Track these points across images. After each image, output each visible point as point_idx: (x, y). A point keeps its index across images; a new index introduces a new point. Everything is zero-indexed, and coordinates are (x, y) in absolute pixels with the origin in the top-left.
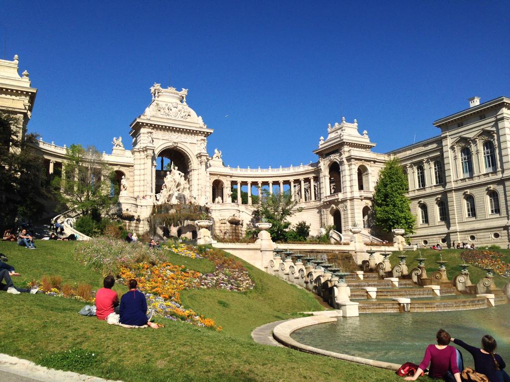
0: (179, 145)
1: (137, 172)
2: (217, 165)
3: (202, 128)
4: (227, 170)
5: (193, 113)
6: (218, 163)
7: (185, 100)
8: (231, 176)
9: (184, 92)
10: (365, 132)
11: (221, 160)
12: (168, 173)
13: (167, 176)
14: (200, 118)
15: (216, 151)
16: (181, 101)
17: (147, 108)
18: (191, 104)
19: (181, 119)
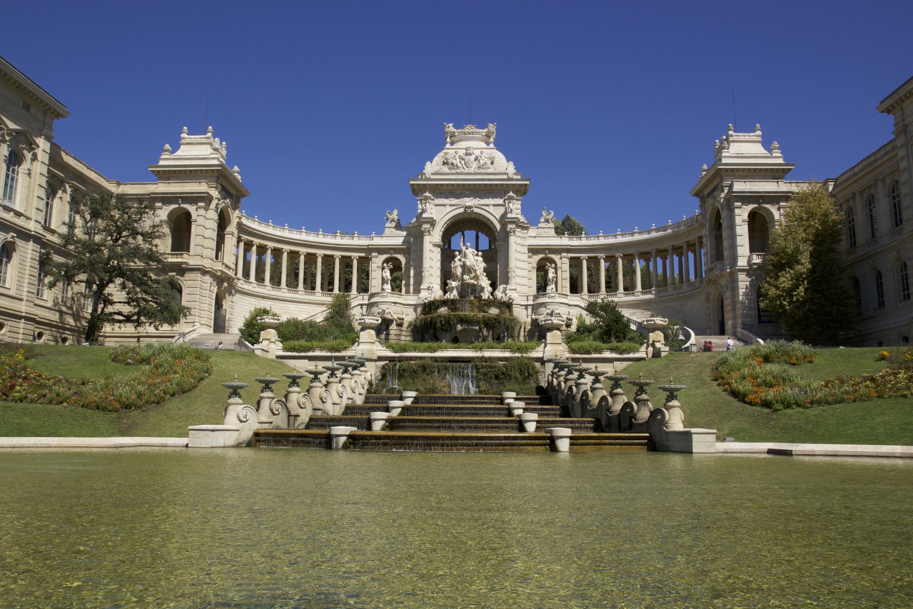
0: (476, 210)
1: (413, 256)
2: (545, 235)
3: (512, 179)
4: (564, 241)
5: (499, 157)
6: (547, 230)
7: (492, 140)
8: (568, 250)
9: (492, 127)
10: (776, 144)
11: (552, 225)
13: (456, 259)
14: (511, 164)
15: (544, 214)
16: (488, 144)
17: (428, 163)
18: (499, 147)
19: (481, 171)
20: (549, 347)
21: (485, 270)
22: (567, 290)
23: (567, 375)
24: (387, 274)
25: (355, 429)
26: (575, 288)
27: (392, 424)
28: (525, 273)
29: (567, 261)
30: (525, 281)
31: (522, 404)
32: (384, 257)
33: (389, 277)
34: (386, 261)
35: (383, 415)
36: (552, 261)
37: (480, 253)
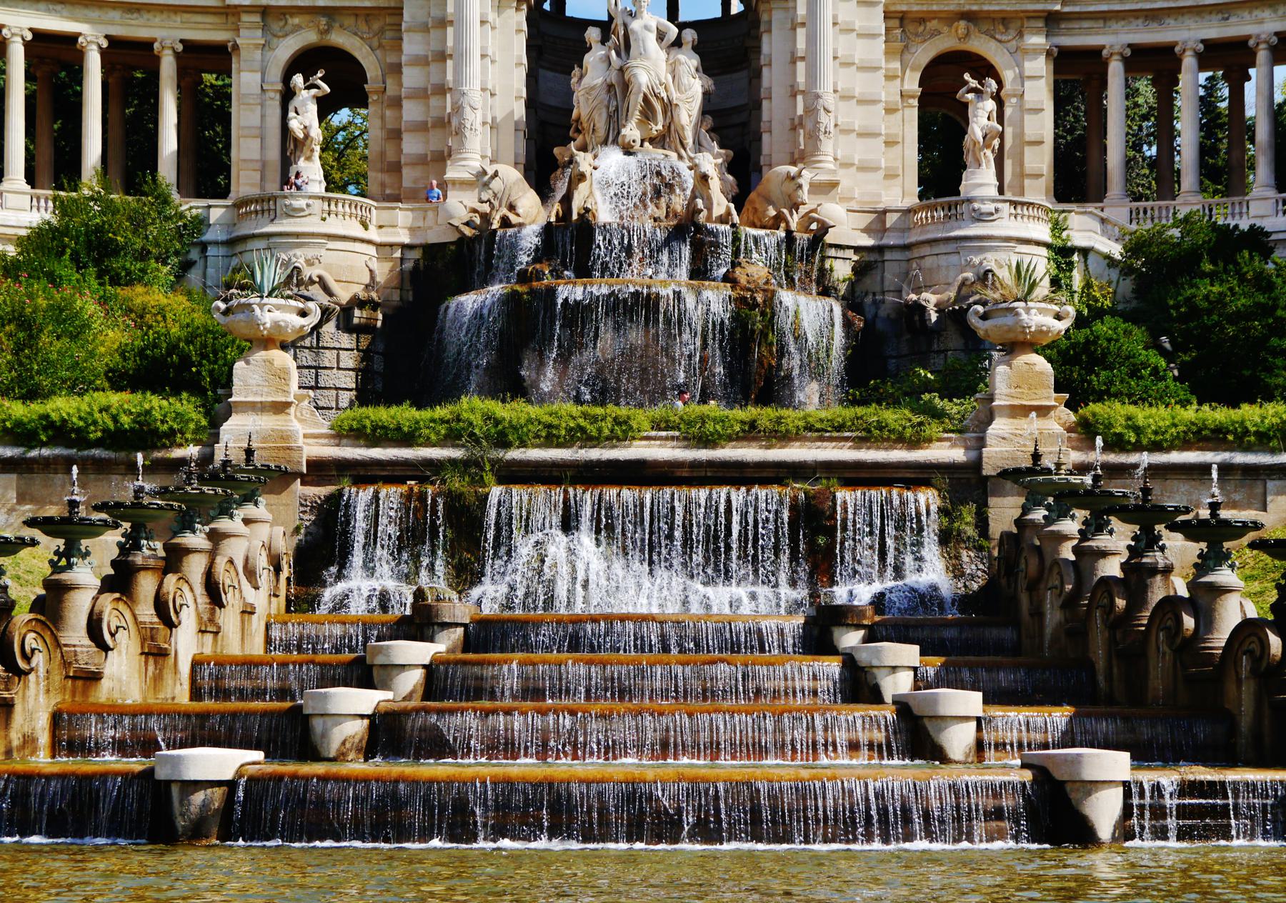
1: (412, 45)
12: (593, 34)
13: (592, 59)
20: (999, 426)
21: (710, 107)
22: (1039, 191)
23: (1084, 535)
24: (305, 118)
25: (258, 755)
26: (1075, 178)
27: (385, 733)
28: (875, 118)
29: (1040, 67)
30: (874, 151)
31: (909, 654)
32: (287, 48)
33: (317, 133)
34: (304, 62)
35: (365, 700)
36: (984, 69)
37: (690, 35)
